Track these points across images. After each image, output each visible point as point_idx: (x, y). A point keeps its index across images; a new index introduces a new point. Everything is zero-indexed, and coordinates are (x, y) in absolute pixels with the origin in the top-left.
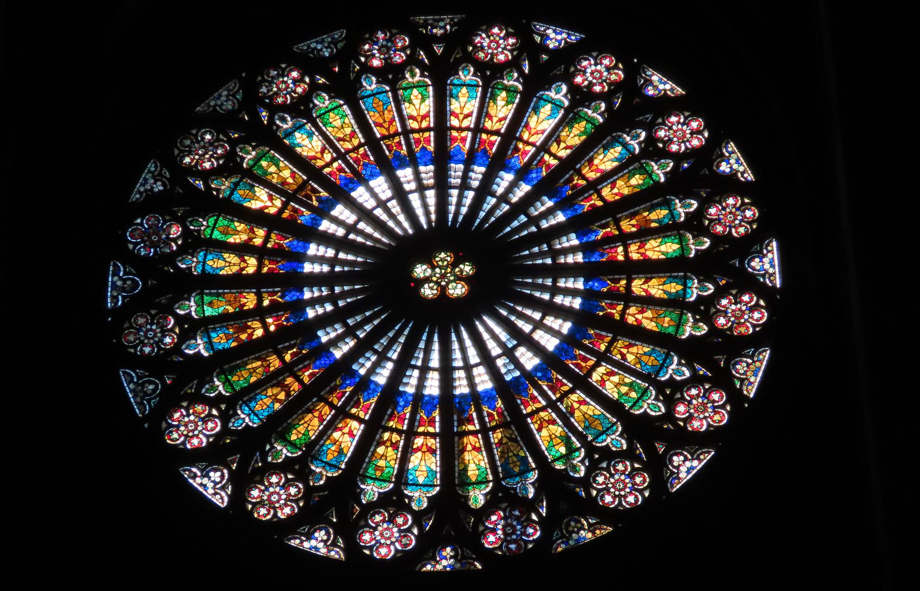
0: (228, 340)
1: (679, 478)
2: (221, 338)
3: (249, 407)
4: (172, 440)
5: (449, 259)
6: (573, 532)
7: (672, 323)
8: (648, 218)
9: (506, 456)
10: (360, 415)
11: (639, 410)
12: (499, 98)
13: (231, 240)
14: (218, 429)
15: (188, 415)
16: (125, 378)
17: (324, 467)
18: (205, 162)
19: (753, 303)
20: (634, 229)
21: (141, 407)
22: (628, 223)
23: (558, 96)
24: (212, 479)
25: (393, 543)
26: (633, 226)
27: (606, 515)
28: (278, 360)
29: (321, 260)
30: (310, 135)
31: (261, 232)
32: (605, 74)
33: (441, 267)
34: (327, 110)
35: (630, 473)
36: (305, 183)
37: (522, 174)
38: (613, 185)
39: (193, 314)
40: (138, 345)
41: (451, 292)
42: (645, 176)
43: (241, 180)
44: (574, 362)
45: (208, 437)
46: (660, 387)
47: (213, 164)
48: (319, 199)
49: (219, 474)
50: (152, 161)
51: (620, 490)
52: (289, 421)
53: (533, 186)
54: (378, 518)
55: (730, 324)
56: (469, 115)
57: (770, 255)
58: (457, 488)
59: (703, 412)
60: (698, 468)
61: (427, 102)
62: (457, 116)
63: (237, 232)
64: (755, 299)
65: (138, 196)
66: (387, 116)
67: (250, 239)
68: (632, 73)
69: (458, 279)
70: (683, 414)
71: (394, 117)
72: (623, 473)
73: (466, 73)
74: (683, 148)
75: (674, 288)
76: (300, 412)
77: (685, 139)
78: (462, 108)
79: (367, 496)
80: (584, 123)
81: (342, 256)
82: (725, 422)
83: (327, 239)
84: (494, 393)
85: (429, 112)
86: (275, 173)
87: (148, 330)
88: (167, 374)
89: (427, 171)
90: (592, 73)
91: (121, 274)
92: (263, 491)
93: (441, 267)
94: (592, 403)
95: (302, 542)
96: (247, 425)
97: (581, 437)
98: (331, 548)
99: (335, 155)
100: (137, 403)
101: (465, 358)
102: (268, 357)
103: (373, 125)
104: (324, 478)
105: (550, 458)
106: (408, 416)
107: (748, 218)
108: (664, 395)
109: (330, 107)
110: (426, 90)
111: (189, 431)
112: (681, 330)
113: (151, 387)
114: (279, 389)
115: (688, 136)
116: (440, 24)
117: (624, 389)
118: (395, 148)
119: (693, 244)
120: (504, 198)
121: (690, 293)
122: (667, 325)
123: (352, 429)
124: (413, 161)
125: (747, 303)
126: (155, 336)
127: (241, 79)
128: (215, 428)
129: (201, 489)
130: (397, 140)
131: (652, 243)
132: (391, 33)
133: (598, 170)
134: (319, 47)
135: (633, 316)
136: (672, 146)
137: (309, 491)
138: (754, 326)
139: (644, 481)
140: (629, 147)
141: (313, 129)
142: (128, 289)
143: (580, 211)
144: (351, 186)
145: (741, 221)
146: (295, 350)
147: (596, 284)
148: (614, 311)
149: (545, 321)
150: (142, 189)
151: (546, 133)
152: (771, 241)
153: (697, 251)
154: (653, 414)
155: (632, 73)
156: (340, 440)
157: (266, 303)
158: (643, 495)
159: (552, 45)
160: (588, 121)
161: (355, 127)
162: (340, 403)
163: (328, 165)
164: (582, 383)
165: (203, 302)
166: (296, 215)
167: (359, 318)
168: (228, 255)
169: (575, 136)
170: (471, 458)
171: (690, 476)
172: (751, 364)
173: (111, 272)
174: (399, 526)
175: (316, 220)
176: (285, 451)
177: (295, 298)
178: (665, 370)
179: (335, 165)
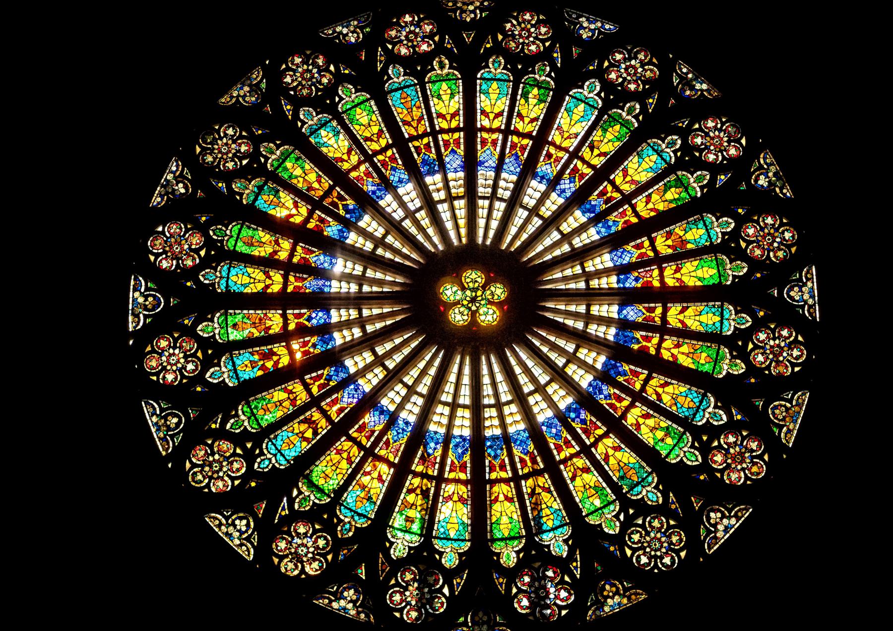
0: (253, 368)
1: (715, 538)
2: (246, 366)
3: (275, 445)
4: (196, 482)
6: (608, 597)
8: (684, 238)
9: (539, 508)
10: (389, 458)
11: (675, 459)
12: (530, 95)
13: (256, 253)
14: (243, 470)
15: (213, 454)
16: (147, 409)
17: (352, 517)
18: (228, 162)
19: (792, 339)
20: (670, 251)
22: (664, 244)
23: (591, 95)
24: (238, 527)
26: (669, 246)
28: (305, 392)
31: (286, 245)
32: (640, 70)
34: (353, 104)
35: (667, 530)
36: (331, 188)
38: (649, 197)
39: (217, 337)
40: (160, 371)
41: (482, 318)
42: (681, 189)
43: (265, 183)
44: (609, 402)
45: (233, 479)
47: (236, 164)
48: (345, 207)
49: (244, 522)
51: (656, 551)
53: (567, 199)
54: (408, 576)
55: (768, 362)
56: (500, 114)
57: (809, 284)
59: (741, 463)
60: (736, 527)
61: (456, 98)
62: (487, 115)
63: (261, 244)
64: (794, 334)
65: (159, 199)
66: (416, 113)
67: (275, 252)
69: (490, 303)
70: (720, 465)
71: (423, 115)
72: (659, 530)
73: (496, 65)
74: (720, 158)
77: (723, 148)
79: (397, 551)
80: (617, 127)
81: (370, 273)
82: (763, 474)
83: (354, 253)
86: (300, 176)
89: (457, 178)
90: (626, 69)
91: (142, 290)
94: (626, 449)
95: (331, 601)
97: (615, 488)
99: (362, 158)
100: (160, 439)
101: (496, 395)
102: (294, 388)
103: (401, 124)
104: (353, 530)
106: (438, 460)
107: (787, 241)
109: (356, 101)
111: (214, 472)
113: (175, 420)
114: (307, 425)
115: (725, 144)
116: (469, 7)
117: (660, 434)
118: (423, 151)
119: (730, 269)
120: (534, 211)
121: (728, 325)
123: (382, 474)
126: (178, 362)
127: (265, 68)
130: (425, 140)
131: (689, 266)
132: (419, 17)
133: (633, 182)
134: (345, 31)
135: (669, 349)
136: (709, 155)
137: (338, 544)
138: (793, 365)
139: (681, 540)
141: (339, 127)
142: (150, 307)
143: (613, 229)
144: (378, 194)
146: (322, 381)
147: (632, 313)
148: (649, 345)
149: (578, 355)
151: (580, 137)
152: (811, 268)
154: (689, 463)
155: (667, 68)
156: (369, 486)
157: (292, 327)
158: (679, 557)
162: (369, 443)
163: (355, 168)
165: (227, 323)
166: (322, 225)
167: (389, 346)
168: (252, 270)
169: (609, 141)
170: (503, 510)
171: (728, 535)
172: (790, 408)
173: (132, 287)
175: (343, 232)
176: (312, 498)
177: (323, 321)
178: (702, 413)
179: (363, 168)
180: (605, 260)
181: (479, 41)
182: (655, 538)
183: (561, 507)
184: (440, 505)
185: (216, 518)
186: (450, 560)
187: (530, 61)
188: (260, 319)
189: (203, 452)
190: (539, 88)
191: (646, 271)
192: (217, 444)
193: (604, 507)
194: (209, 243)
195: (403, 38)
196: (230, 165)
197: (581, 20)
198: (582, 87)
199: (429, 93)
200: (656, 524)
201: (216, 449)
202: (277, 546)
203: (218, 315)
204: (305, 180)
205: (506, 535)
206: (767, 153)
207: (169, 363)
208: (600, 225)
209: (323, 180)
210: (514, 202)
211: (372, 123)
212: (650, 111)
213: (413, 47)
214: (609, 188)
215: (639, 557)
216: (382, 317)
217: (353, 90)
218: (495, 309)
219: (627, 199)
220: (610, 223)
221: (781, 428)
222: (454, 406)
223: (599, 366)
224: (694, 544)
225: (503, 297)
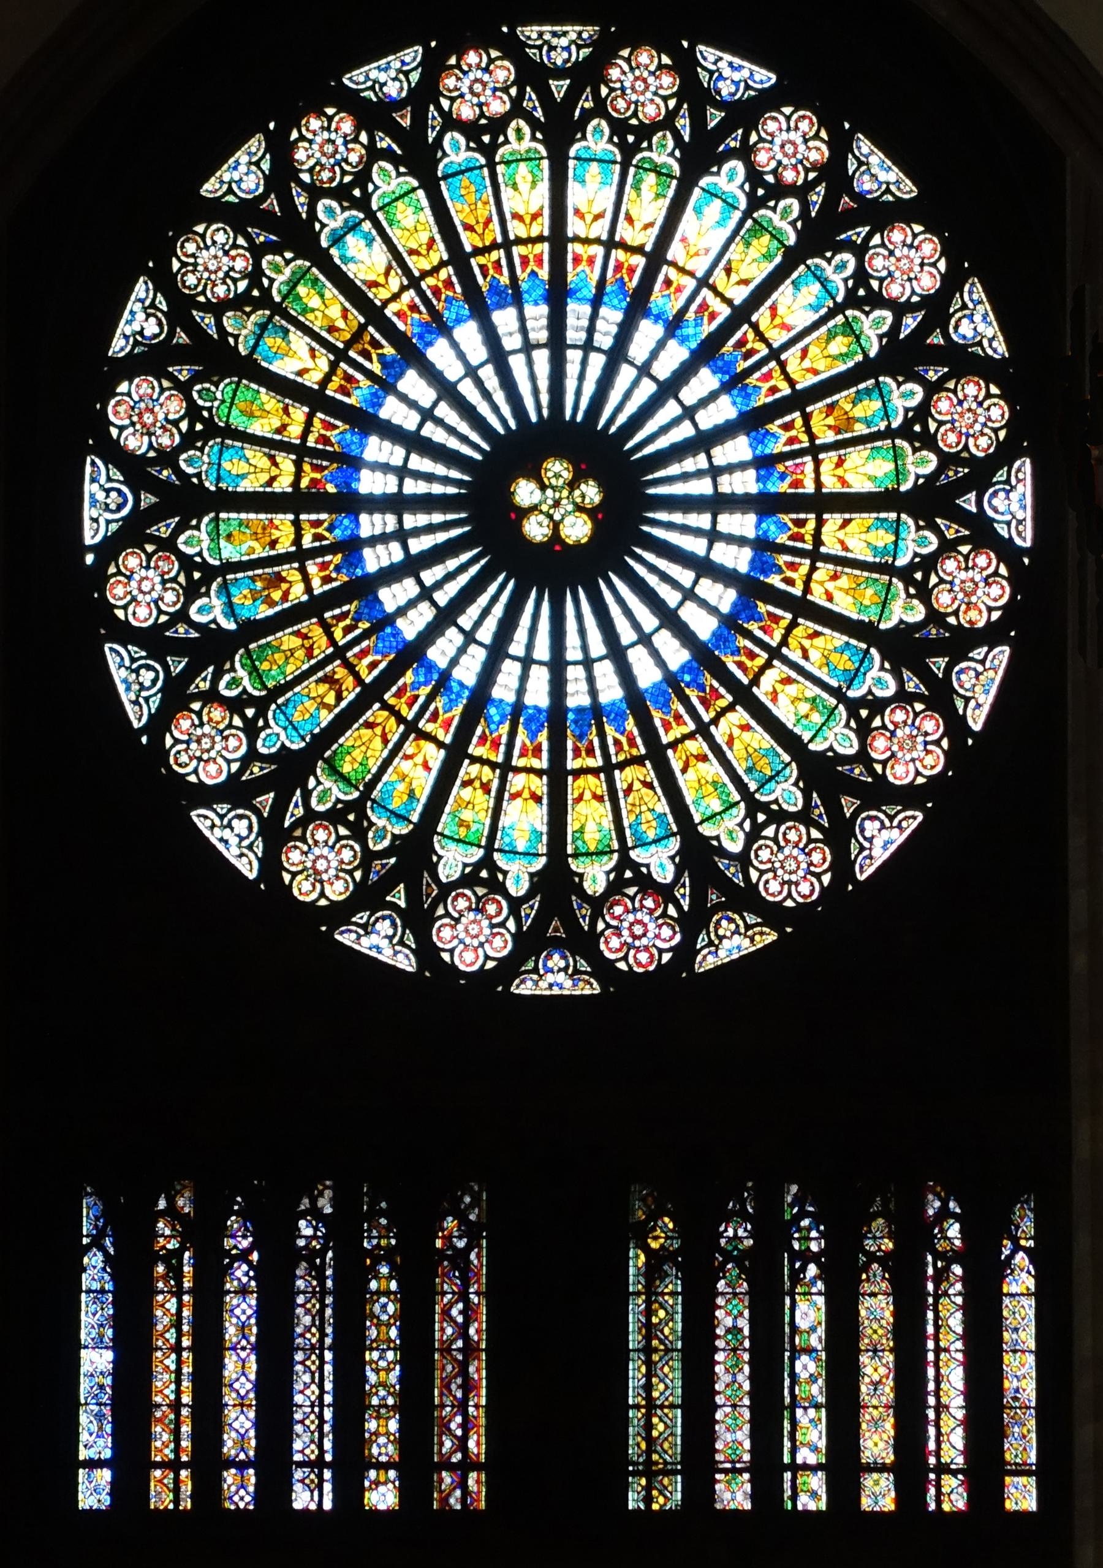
1: (870, 857)
3: (284, 714)
4: (180, 765)
5: (565, 474)
7: (876, 599)
8: (851, 415)
12: (644, 187)
15: (202, 725)
17: (389, 819)
19: (991, 570)
21: (137, 708)
24: (236, 831)
25: (481, 945)
26: (830, 427)
27: (772, 914)
29: (386, 468)
30: (370, 242)
31: (299, 413)
32: (802, 148)
33: (554, 488)
35: (806, 846)
36: (362, 328)
37: (674, 325)
38: (805, 352)
44: (737, 658)
45: (229, 762)
46: (853, 707)
49: (245, 822)
50: (141, 279)
51: (790, 873)
52: (341, 741)
53: (693, 353)
54: (462, 904)
57: (1020, 487)
58: (570, 860)
59: (910, 751)
64: (994, 562)
65: (122, 342)
66: (482, 212)
68: (840, 146)
69: (579, 508)
72: (796, 845)
73: (597, 136)
74: (908, 292)
75: (884, 538)
76: (356, 726)
77: (912, 275)
78: (591, 202)
83: (392, 432)
84: (624, 706)
85: (542, 208)
87: (143, 579)
88: (172, 655)
89: (538, 314)
91: (103, 479)
92: (306, 853)
93: (554, 488)
95: (359, 937)
96: (283, 745)
98: (398, 948)
99: (406, 282)
103: (460, 229)
104: (389, 836)
105: (697, 819)
106: (504, 740)
108: (858, 718)
110: (538, 166)
112: (887, 610)
113: (151, 674)
114: (327, 686)
115: (917, 269)
122: (867, 602)
124: (517, 300)
125: (983, 569)
126: (153, 589)
127: (269, 136)
128: (238, 748)
129: (221, 847)
130: (494, 255)
131: (856, 456)
132: (488, 55)
134: (383, 77)
137: (368, 858)
138: (990, 610)
139: (824, 860)
140: (829, 286)
141: (374, 232)
144: (428, 337)
145: (985, 425)
146: (348, 622)
147: (773, 528)
150: (128, 332)
153: (918, 477)
155: (840, 146)
159: (726, 89)
160: (773, 236)
161: (435, 230)
163: (395, 297)
164: (744, 697)
165: (218, 535)
174: (490, 918)
176: (335, 790)
177: (349, 532)
180: (738, 449)
181: (573, 95)
182: (790, 856)
183: (667, 811)
184: (505, 803)
185: (206, 817)
186: (518, 886)
187: (646, 132)
188: (264, 529)
189: (189, 722)
190: (659, 174)
191: (797, 465)
192: (206, 710)
193: (724, 811)
194: (193, 412)
195: (465, 90)
196: (221, 290)
197: (720, 64)
198: (718, 173)
199: (500, 179)
200: (792, 836)
201: (205, 719)
202: (288, 859)
203: (206, 520)
204: (325, 315)
205: (592, 849)
206: (973, 284)
207: (141, 591)
208: (735, 392)
209: (350, 317)
210: (617, 355)
211: (419, 227)
212: (813, 214)
213: (480, 105)
214: (751, 336)
215: (767, 882)
216: (430, 529)
217: (394, 174)
218: (585, 517)
219: (775, 354)
220: (750, 391)
221: (967, 700)
222: (527, 662)
223: (725, 608)
224: (842, 866)
225: (597, 499)
